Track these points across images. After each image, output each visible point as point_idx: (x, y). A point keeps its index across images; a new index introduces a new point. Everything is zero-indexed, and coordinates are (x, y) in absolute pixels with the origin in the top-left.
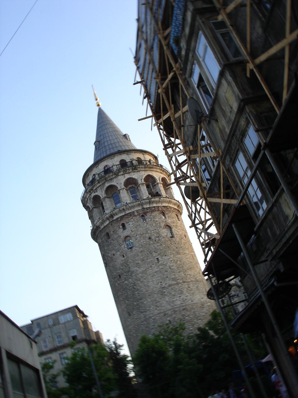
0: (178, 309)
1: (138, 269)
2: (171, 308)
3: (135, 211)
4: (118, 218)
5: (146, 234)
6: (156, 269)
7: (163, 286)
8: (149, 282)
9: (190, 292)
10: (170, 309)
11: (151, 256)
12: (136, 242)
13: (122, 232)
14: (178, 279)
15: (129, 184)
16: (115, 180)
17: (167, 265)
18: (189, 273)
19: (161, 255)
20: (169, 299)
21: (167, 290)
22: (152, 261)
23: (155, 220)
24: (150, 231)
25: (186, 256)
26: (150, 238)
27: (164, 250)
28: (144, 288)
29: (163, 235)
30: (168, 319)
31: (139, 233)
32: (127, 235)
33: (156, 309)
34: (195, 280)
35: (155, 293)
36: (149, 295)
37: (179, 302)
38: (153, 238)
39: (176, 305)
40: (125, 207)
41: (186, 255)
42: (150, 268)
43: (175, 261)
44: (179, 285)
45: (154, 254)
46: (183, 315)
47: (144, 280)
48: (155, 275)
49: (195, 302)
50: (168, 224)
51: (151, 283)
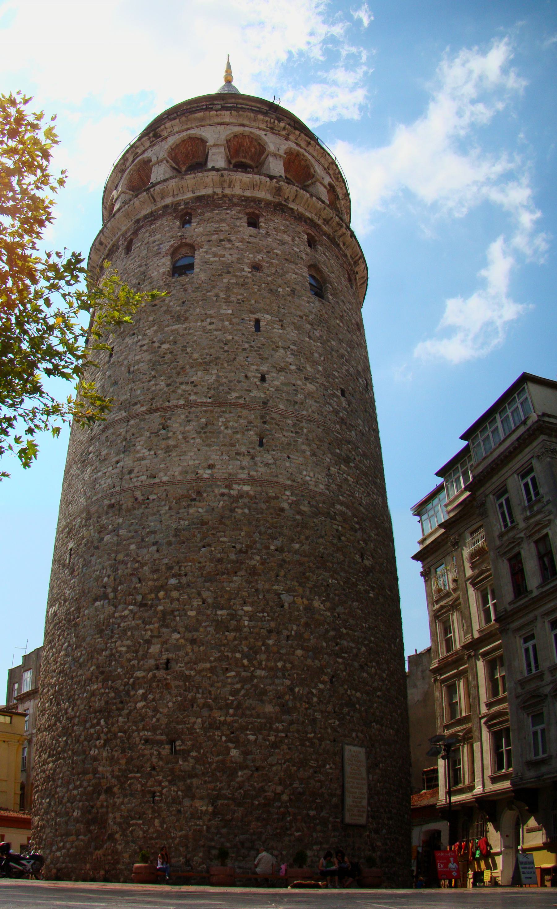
25: (211, 324)
34: (209, 400)
41: (214, 320)
44: (132, 422)
49: (165, 479)
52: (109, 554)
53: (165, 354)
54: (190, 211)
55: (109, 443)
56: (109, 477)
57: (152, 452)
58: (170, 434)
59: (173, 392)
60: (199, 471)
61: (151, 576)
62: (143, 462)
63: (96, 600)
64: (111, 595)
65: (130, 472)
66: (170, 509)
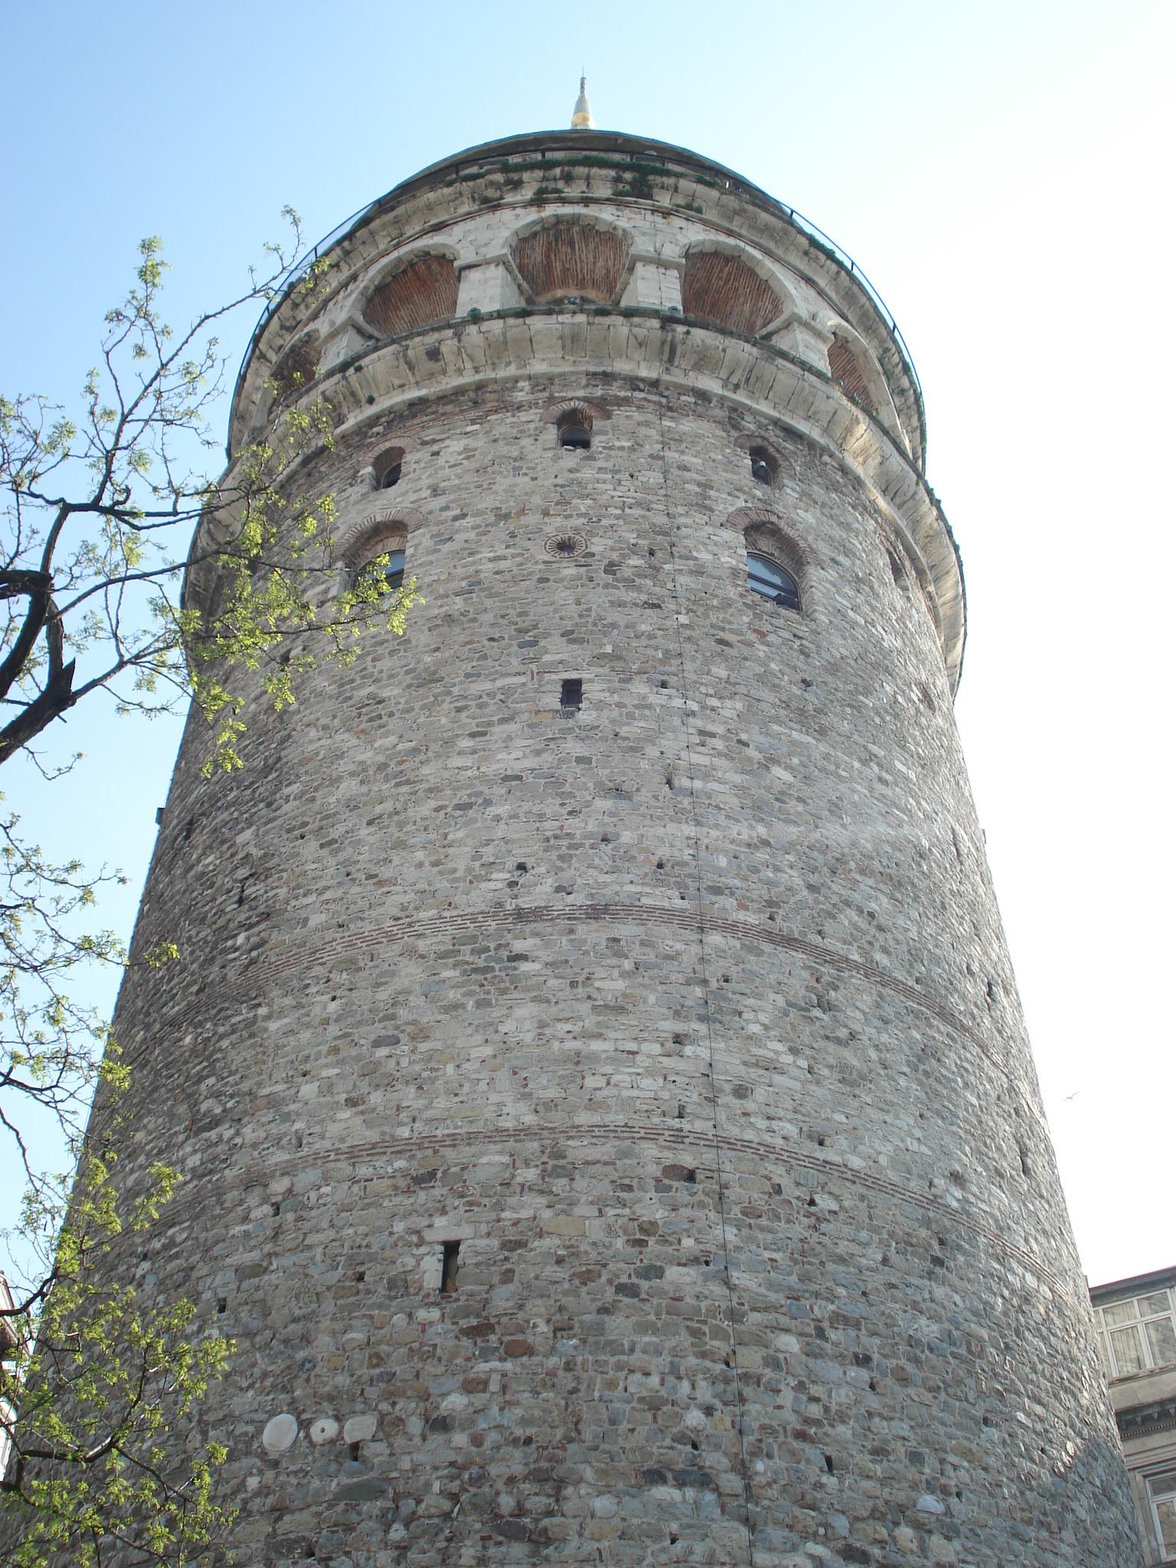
0: (606, 1150)
1: (355, 741)
2: (530, 1119)
3: (530, 378)
4: (374, 421)
5: (546, 513)
6: (514, 758)
7: (525, 902)
8: (400, 845)
9: (831, 1047)
10: (508, 1123)
11: (515, 662)
12: (431, 558)
13: (356, 503)
14: (717, 891)
15: (564, 284)
16: (458, 230)
17: (652, 751)
18: (873, 906)
19: (619, 665)
20: (542, 1025)
21: (547, 944)
22: (507, 691)
23: (671, 455)
24: (589, 502)
26: (565, 547)
27: (659, 641)
28: (328, 895)
29: (704, 556)
30: (443, 1228)
31: (488, 502)
32: (378, 519)
33: (351, 1102)
34: (918, 987)
35: (411, 953)
36: (350, 965)
37: (650, 1085)
38: (593, 549)
39: (592, 1104)
40: (450, 333)
42: (465, 743)
43: (751, 752)
44: (715, 939)
45: (556, 650)
46: (649, 1228)
47: (364, 832)
48: (488, 803)
49: (856, 1162)
50: (782, 524)
51: (420, 855)
52: (695, 1333)
53: (782, 793)
54: (771, 450)
55: (628, 965)
56: (650, 1073)
57: (803, 1064)
58: (843, 1033)
59: (834, 917)
60: (936, 1181)
61: (864, 1460)
62: (777, 1079)
63: (655, 1476)
64: (732, 1482)
65: (741, 1092)
66: (885, 1261)
